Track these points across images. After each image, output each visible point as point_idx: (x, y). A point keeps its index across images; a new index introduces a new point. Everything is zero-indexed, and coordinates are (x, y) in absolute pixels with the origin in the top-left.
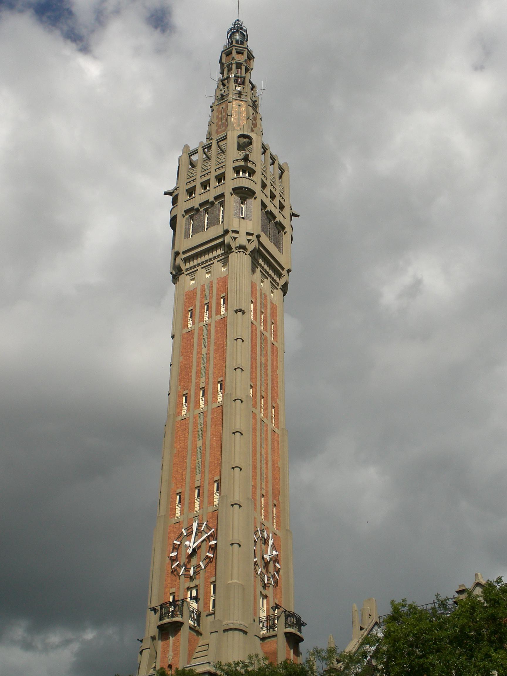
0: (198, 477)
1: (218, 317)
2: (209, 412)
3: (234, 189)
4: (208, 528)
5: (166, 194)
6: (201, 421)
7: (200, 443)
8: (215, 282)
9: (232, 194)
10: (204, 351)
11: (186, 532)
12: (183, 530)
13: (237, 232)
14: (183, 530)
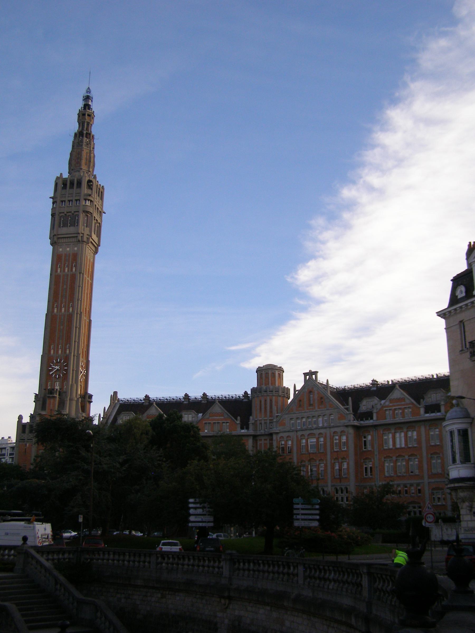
0: (61, 341)
1: (72, 273)
2: (66, 316)
3: (83, 211)
4: (64, 362)
5: (50, 198)
6: (62, 318)
7: (62, 327)
8: (71, 254)
9: (82, 213)
10: (65, 287)
11: (56, 362)
12: (54, 360)
13: (83, 234)
14: (54, 360)
